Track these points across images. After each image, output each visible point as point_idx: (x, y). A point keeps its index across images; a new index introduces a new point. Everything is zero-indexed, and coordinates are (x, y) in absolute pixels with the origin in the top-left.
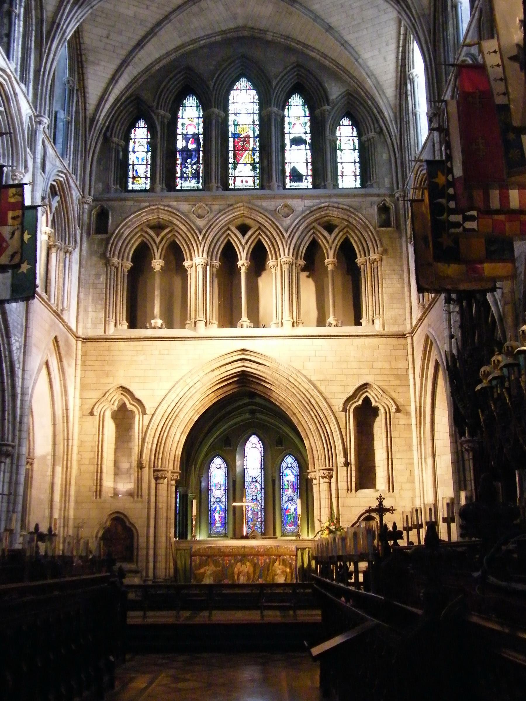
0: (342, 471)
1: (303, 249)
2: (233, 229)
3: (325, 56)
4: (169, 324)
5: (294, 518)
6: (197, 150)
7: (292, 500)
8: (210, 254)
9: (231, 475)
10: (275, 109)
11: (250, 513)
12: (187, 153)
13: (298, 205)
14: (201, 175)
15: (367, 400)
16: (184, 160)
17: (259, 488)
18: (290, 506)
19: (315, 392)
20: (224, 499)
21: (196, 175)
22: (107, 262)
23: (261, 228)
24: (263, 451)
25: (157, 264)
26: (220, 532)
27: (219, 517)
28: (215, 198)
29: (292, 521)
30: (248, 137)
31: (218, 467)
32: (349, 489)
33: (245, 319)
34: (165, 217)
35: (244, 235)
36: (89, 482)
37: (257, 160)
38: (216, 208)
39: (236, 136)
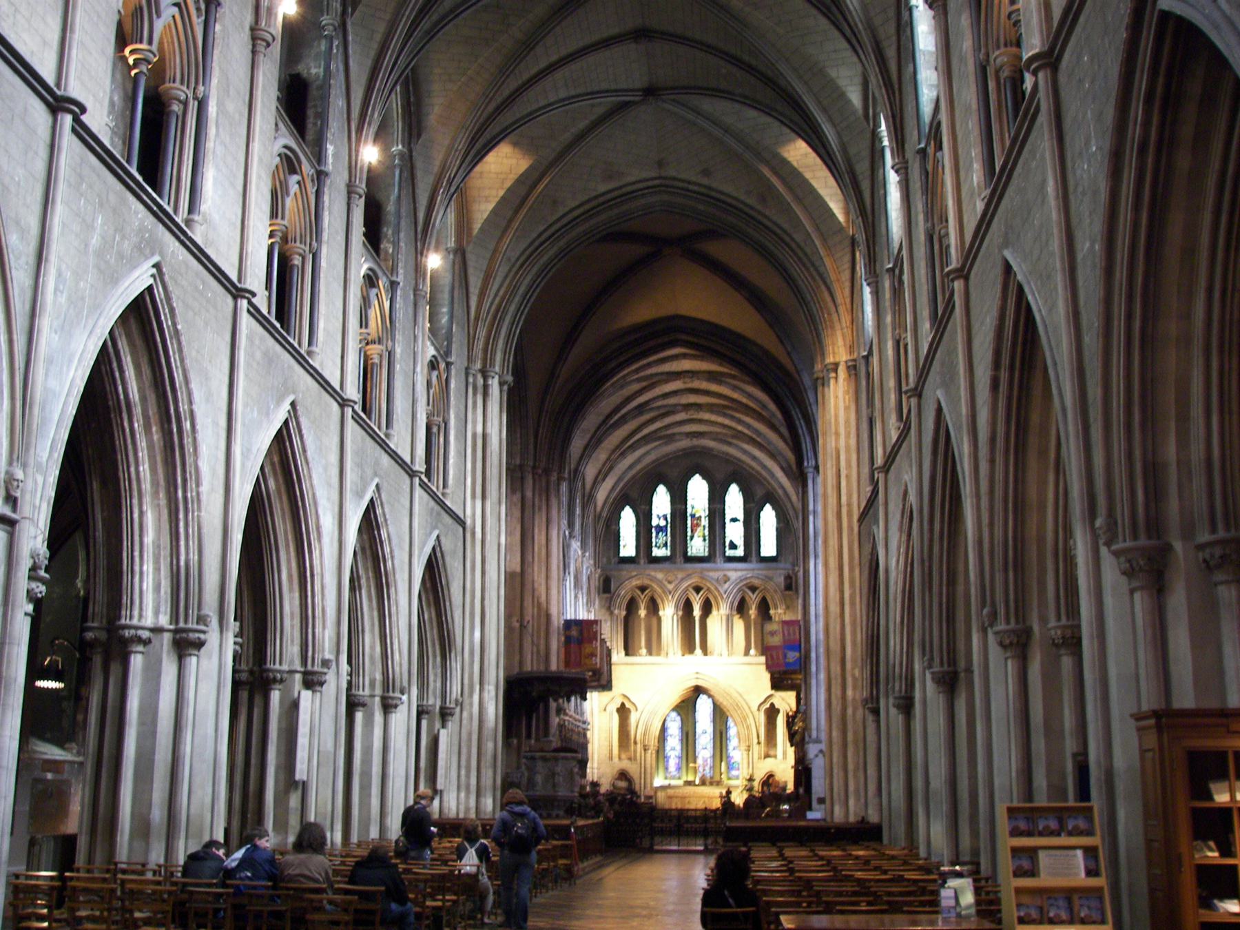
0: (756, 748)
1: (736, 604)
2: (691, 590)
3: (753, 469)
4: (650, 653)
6: (666, 526)
8: (677, 607)
9: (685, 728)
10: (719, 506)
12: (660, 529)
13: (733, 575)
14: (669, 544)
15: (772, 705)
16: (657, 533)
19: (740, 699)
21: (665, 545)
22: (611, 613)
23: (708, 589)
25: (642, 613)
28: (679, 569)
30: (700, 517)
32: (760, 758)
33: (698, 651)
34: (646, 582)
35: (698, 593)
36: (606, 752)
37: (707, 533)
38: (680, 576)
39: (693, 516)
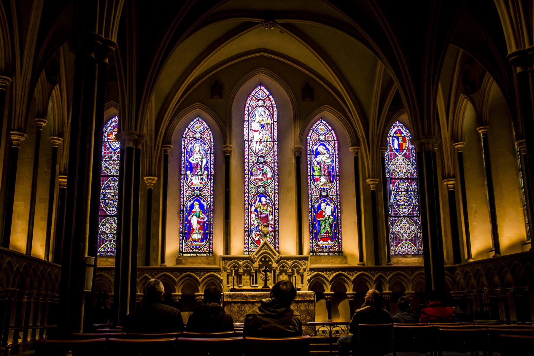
5: (331, 225)
7: (327, 195)
11: (253, 216)
17: (269, 175)
18: (323, 205)
20: (206, 192)
24: (275, 113)
26: (200, 248)
27: (199, 222)
29: (327, 232)
31: (198, 136)
